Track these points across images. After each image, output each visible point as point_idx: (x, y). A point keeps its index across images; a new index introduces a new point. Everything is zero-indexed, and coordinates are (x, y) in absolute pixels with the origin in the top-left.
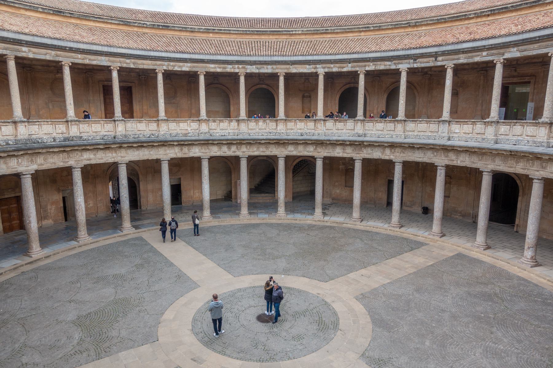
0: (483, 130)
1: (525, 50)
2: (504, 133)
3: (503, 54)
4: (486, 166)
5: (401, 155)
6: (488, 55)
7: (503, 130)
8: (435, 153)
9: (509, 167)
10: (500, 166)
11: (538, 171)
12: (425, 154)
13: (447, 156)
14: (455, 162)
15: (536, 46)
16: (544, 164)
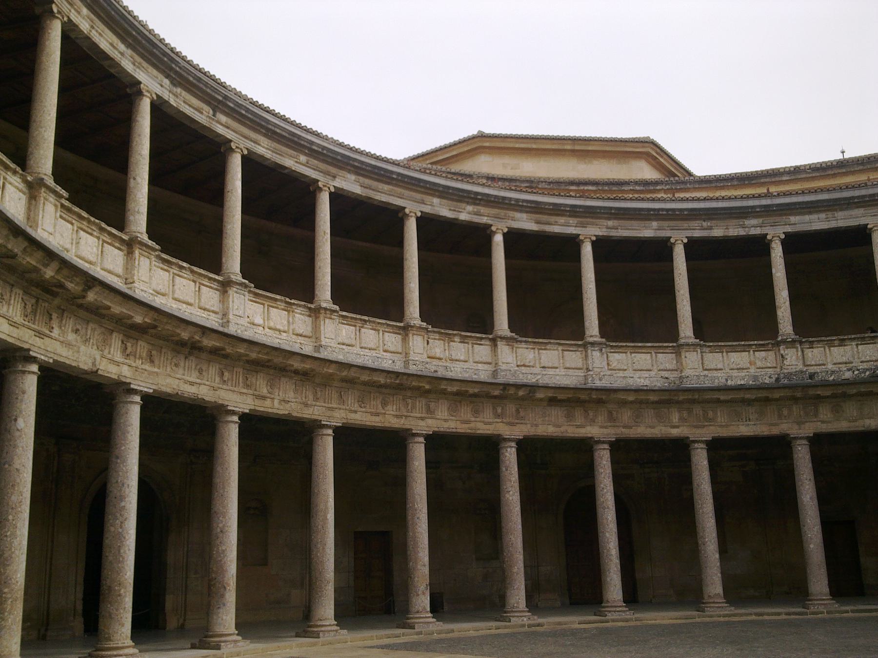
0: (310, 329)
1: (369, 188)
2: (346, 341)
3: (334, 177)
4: (329, 413)
5: (144, 367)
6: (306, 165)
7: (344, 331)
8: (227, 375)
9: (372, 414)
10: (356, 412)
11: (422, 419)
12: (200, 371)
13: (248, 386)
14: (268, 403)
15: (386, 187)
16: (432, 405)
